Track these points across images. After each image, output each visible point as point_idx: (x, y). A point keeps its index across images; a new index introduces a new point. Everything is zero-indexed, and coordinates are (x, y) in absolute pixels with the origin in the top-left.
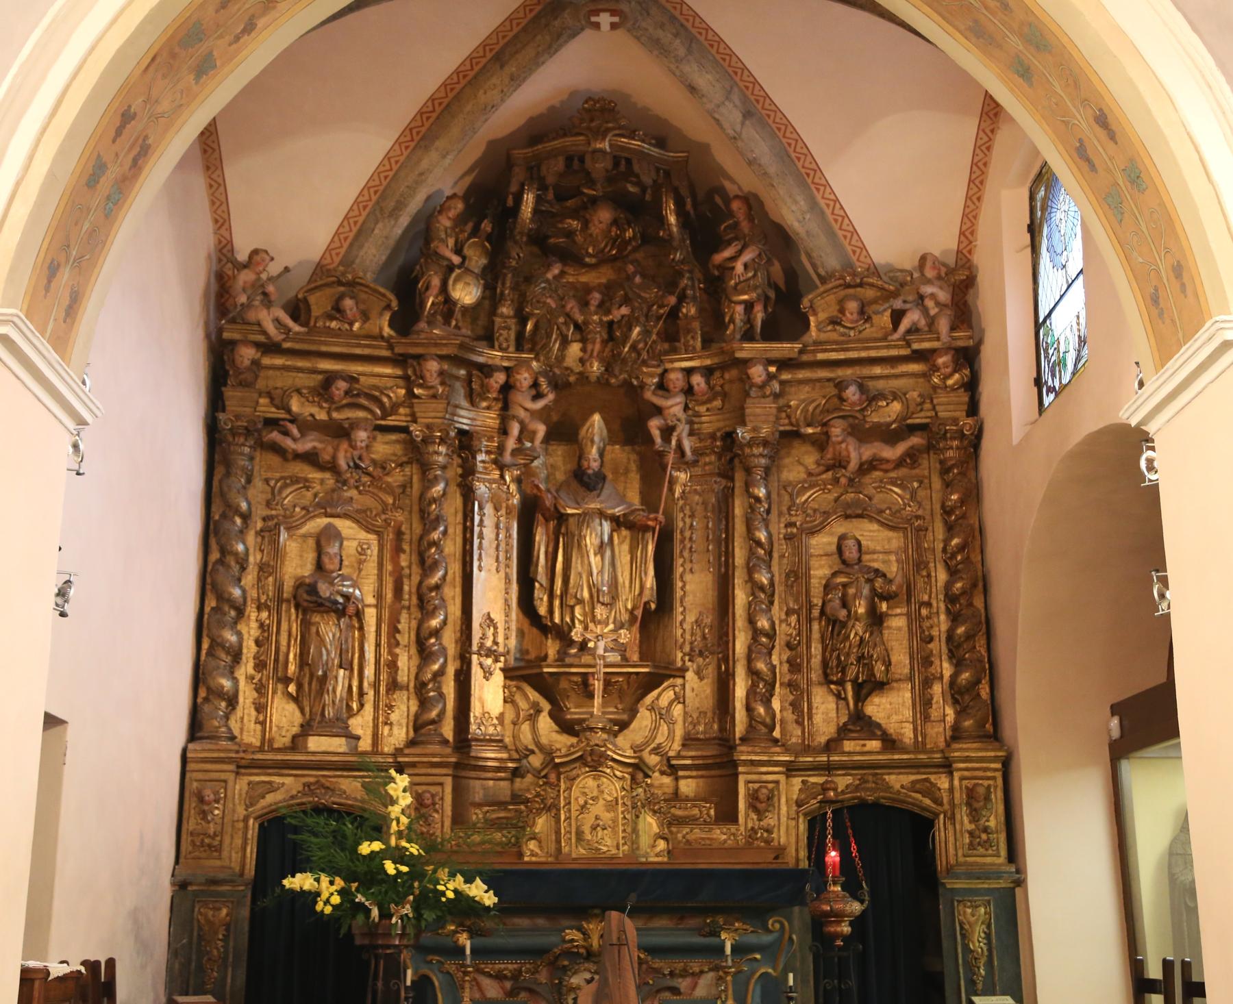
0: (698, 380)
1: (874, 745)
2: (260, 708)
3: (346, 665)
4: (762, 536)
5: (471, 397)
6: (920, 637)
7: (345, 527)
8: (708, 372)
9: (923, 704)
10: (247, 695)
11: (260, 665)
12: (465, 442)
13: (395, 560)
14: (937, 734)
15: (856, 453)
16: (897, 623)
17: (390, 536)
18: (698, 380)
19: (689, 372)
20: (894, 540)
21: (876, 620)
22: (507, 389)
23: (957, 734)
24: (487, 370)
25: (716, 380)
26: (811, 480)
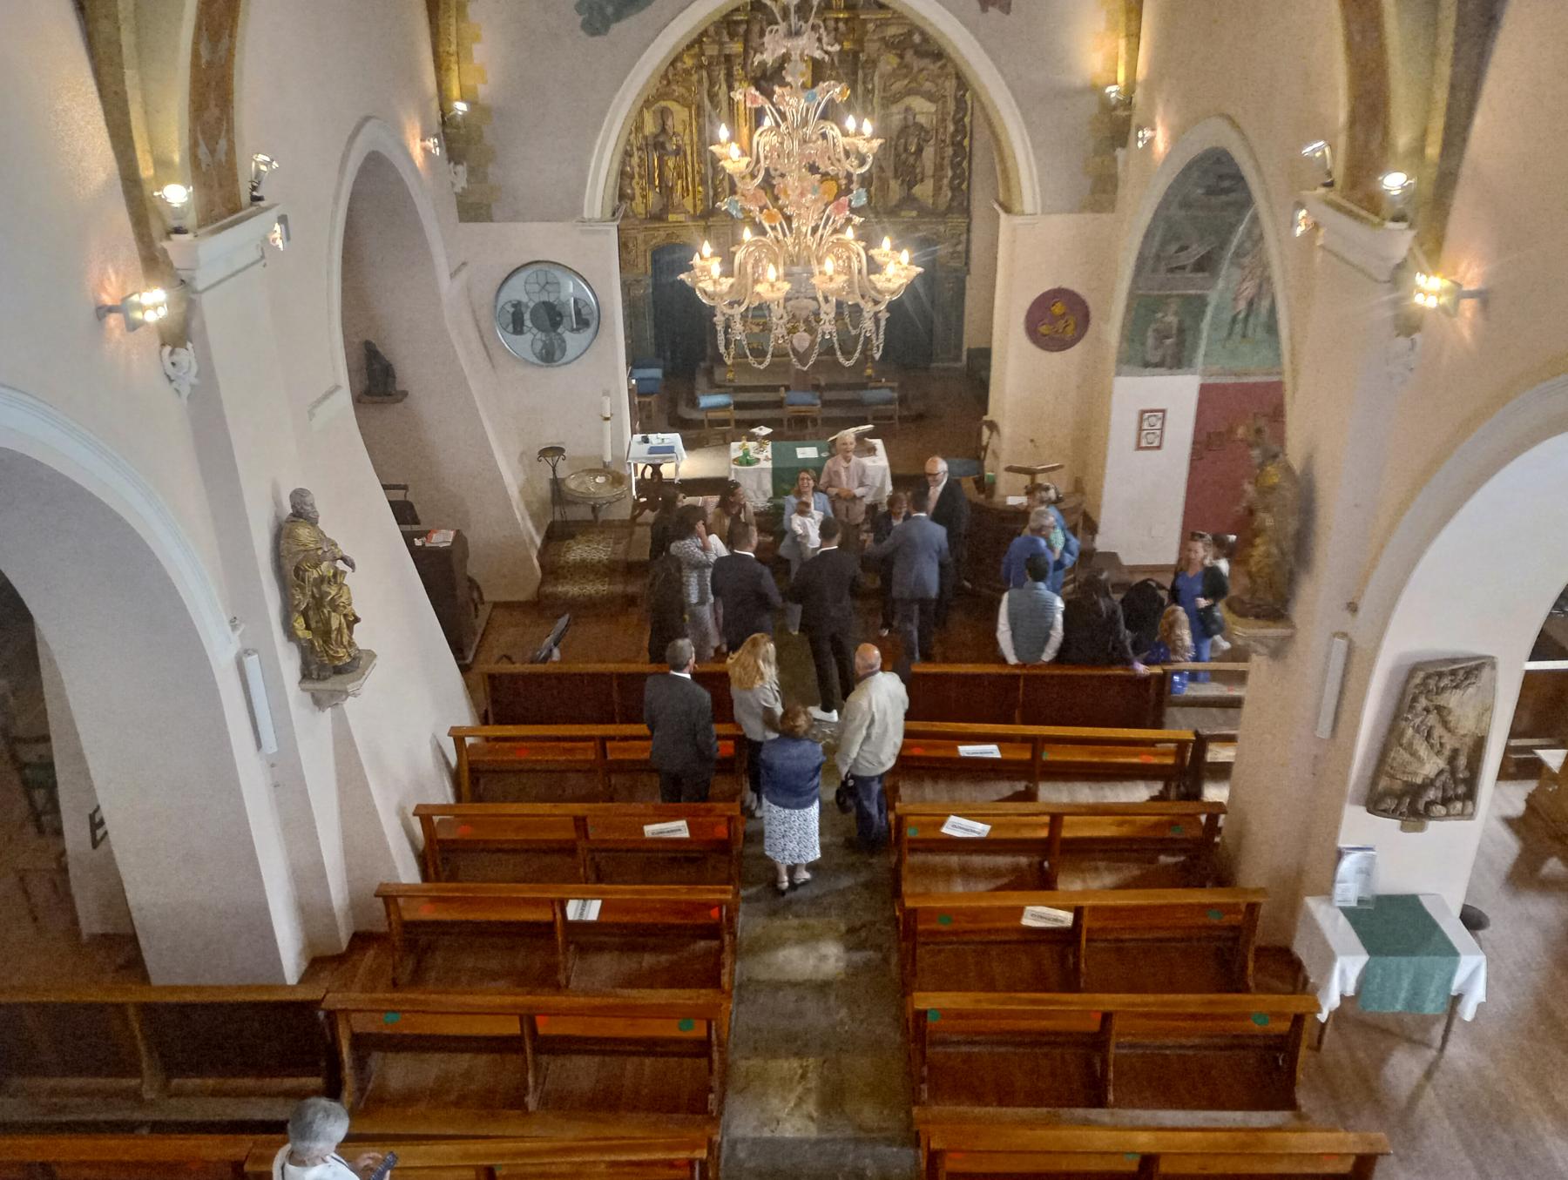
0: (841, 25)
1: (914, 213)
2: (644, 197)
3: (679, 176)
4: (870, 87)
5: (732, 36)
6: (940, 153)
7: (674, 106)
8: (846, 21)
9: (938, 189)
10: (638, 192)
11: (641, 177)
12: (728, 59)
13: (698, 122)
14: (942, 206)
15: (917, 64)
16: (929, 152)
17: (694, 107)
18: (841, 25)
19: (837, 20)
20: (931, 107)
21: (920, 150)
22: (747, 32)
23: (949, 209)
24: (738, 23)
25: (850, 24)
26: (894, 74)
